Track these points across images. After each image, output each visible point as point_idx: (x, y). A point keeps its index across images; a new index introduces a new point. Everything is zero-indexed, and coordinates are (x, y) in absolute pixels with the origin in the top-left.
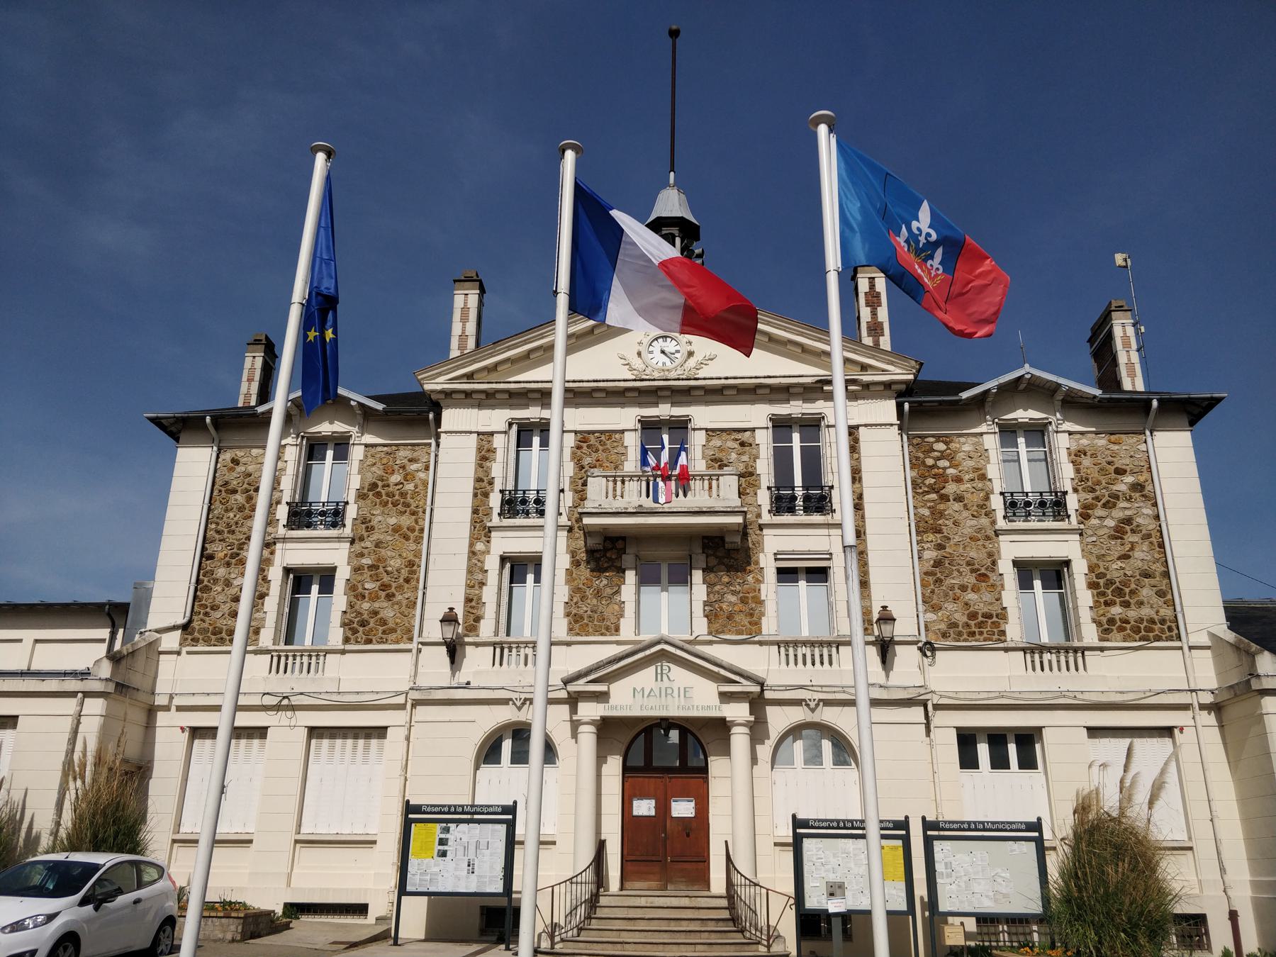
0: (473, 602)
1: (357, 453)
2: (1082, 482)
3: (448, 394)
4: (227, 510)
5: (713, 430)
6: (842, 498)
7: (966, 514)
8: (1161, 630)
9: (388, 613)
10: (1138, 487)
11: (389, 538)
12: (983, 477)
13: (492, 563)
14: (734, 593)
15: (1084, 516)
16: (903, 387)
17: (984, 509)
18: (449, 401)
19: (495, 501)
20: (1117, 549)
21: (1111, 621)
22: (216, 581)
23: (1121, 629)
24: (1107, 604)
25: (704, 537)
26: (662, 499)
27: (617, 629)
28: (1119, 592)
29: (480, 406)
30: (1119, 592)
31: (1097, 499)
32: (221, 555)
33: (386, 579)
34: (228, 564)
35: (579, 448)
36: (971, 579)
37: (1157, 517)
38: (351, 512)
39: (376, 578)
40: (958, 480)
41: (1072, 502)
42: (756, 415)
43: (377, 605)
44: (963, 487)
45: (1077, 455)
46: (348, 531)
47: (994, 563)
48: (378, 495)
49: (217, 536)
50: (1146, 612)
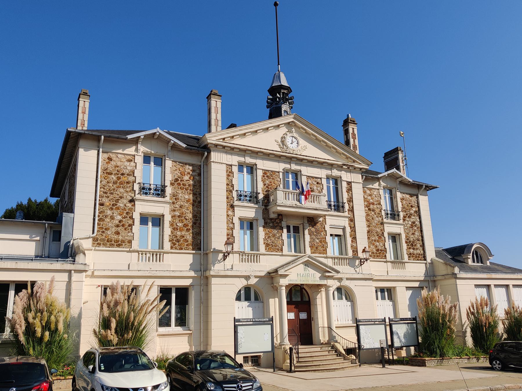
2: (404, 209)
3: (216, 146)
4: (108, 182)
5: (309, 176)
6: (347, 207)
7: (375, 216)
10: (415, 212)
11: (186, 204)
12: (380, 204)
13: (236, 221)
14: (318, 239)
15: (404, 220)
16: (365, 170)
17: (380, 215)
18: (215, 148)
19: (235, 194)
21: (410, 254)
22: (106, 216)
23: (413, 257)
24: (410, 248)
25: (308, 217)
26: (303, 203)
27: (282, 250)
28: (412, 245)
29: (226, 153)
30: (412, 245)
31: (407, 214)
32: (108, 204)
33: (185, 222)
34: (112, 209)
35: (264, 176)
36: (377, 238)
37: (420, 222)
38: (169, 190)
39: (182, 222)
40: (373, 204)
41: (402, 215)
42: (322, 173)
43: (183, 233)
44: (375, 206)
45: (402, 199)
46: (168, 199)
47: (383, 233)
48: (179, 184)
49: (105, 195)
50: (418, 251)
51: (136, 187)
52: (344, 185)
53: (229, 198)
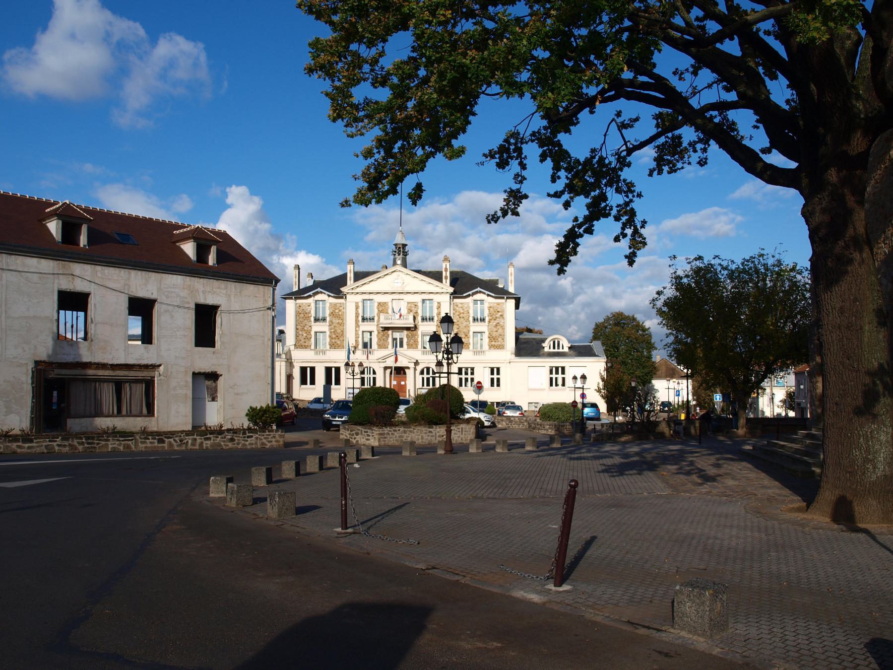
0: (356, 341)
1: (328, 305)
2: (490, 315)
8: (501, 347)
9: (339, 342)
13: (360, 333)
17: (468, 320)
19: (360, 318)
20: (495, 329)
38: (328, 319)
41: (487, 319)
42: (418, 299)
51: (312, 319)
52: (435, 305)
53: (357, 321)
